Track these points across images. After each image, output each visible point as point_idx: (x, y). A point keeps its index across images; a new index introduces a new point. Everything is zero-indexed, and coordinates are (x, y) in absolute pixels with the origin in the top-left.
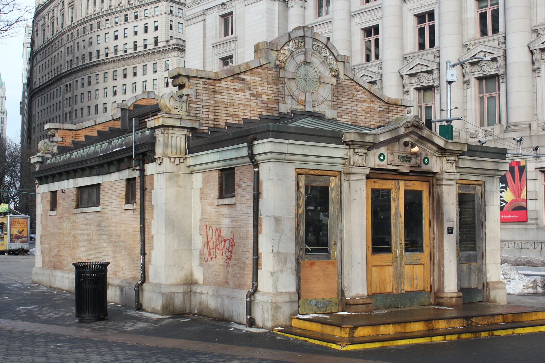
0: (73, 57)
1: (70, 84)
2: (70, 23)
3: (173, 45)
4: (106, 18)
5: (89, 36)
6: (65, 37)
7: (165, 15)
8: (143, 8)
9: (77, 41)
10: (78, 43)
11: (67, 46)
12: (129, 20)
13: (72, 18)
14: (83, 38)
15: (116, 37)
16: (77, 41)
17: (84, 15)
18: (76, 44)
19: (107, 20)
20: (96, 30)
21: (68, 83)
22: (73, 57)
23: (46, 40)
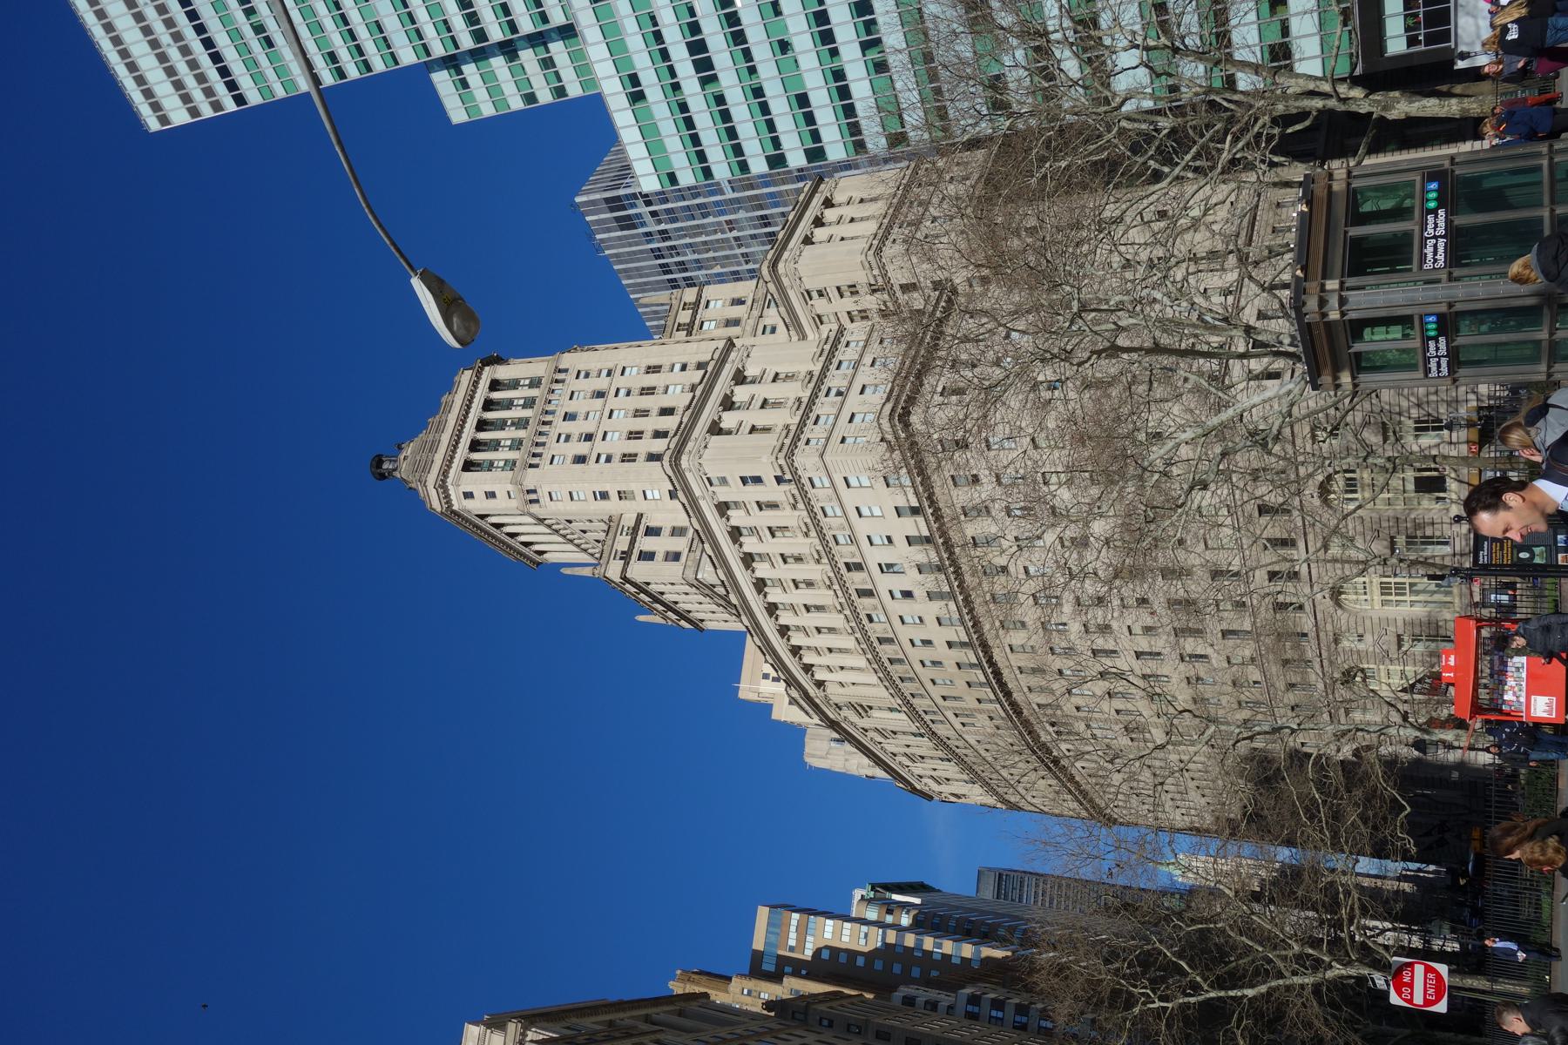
0: (980, 711)
1: (1053, 724)
2: (903, 716)
3: (893, 426)
4: (865, 621)
5: (918, 667)
6: (942, 730)
7: (827, 457)
8: (824, 521)
9: (940, 701)
10: (944, 698)
11: (958, 726)
12: (858, 560)
13: (891, 710)
14: (929, 685)
15: (907, 594)
16: (940, 701)
17: (873, 679)
18: (947, 703)
19: (870, 619)
20: (897, 647)
21: (1051, 729)
22: (980, 711)
23: (965, 777)
